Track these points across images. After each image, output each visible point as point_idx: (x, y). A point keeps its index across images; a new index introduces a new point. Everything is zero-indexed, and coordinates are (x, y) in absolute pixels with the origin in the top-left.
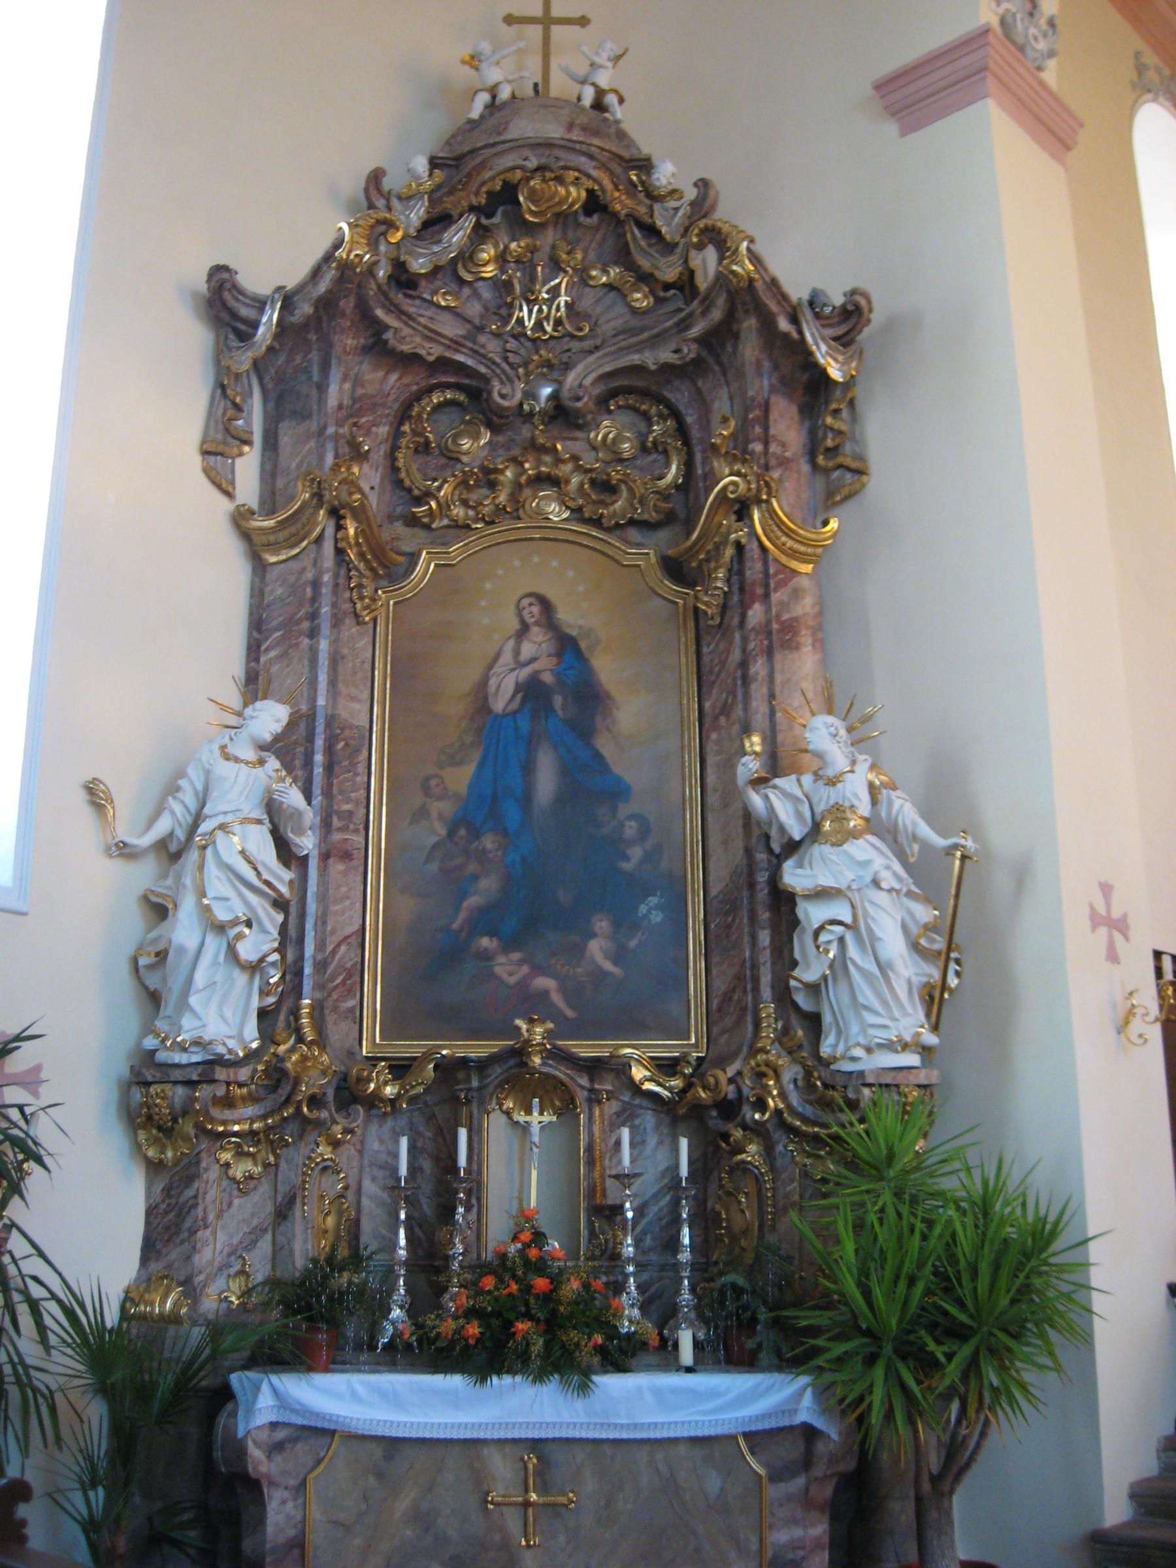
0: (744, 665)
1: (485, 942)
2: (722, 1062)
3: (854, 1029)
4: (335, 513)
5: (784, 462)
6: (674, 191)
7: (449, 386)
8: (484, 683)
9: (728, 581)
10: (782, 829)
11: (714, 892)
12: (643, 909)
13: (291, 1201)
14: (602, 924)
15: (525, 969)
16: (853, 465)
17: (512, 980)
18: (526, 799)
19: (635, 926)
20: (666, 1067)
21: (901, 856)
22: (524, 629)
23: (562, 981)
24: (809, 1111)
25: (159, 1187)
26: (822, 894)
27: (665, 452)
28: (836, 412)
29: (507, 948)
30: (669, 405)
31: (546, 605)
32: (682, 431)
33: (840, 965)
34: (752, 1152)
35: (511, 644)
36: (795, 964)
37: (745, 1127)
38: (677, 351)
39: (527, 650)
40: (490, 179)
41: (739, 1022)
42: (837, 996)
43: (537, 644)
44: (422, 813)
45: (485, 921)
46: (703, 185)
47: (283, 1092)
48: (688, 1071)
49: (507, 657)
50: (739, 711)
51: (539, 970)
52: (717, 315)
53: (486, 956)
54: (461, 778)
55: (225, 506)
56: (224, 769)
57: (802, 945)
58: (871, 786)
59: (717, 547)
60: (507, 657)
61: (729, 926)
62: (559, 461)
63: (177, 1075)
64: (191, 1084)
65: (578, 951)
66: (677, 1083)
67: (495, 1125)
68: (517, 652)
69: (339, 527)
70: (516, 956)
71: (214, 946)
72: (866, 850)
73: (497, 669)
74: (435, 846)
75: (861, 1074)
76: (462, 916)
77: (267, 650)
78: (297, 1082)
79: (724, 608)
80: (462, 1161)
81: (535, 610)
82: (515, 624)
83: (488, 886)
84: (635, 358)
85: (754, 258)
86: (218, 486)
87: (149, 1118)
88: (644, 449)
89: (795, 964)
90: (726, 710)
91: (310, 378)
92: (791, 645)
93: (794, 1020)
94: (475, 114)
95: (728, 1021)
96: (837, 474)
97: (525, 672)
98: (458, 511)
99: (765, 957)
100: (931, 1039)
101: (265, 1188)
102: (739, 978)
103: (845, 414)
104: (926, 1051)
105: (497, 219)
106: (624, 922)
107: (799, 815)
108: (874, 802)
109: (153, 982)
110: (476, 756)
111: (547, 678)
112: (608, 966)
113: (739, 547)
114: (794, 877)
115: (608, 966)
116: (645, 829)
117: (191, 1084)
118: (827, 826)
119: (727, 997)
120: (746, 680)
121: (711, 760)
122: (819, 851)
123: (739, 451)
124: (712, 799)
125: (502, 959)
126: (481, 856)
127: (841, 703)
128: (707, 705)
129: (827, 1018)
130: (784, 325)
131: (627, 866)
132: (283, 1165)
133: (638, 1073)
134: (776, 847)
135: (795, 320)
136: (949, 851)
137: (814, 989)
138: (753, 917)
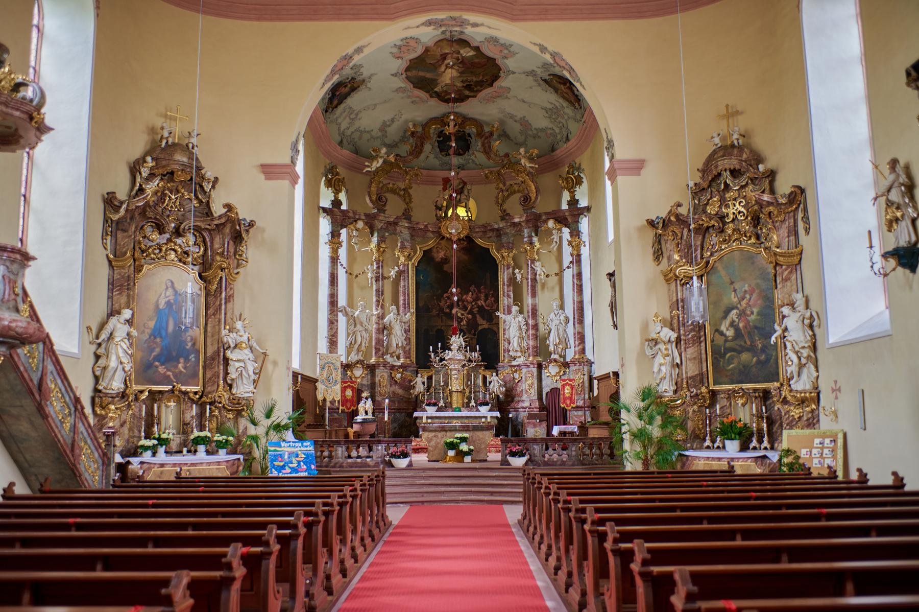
0: (220, 305)
1: (157, 363)
2: (209, 393)
3: (242, 388)
4: (134, 260)
5: (231, 256)
6: (209, 179)
7: (152, 222)
8: (158, 301)
9: (217, 285)
10: (229, 344)
11: (208, 354)
12: (190, 357)
13: (125, 422)
14: (182, 360)
15: (165, 370)
16: (245, 260)
17: (162, 372)
18: (166, 330)
19: (189, 360)
20: (196, 393)
21: (252, 352)
22: (167, 288)
23: (173, 372)
24: (230, 404)
25: (96, 420)
26: (239, 361)
27: (199, 246)
28: (242, 247)
29: (162, 365)
30: (202, 235)
31: (172, 283)
32: (204, 242)
33: (241, 374)
34: (217, 413)
35: (164, 292)
36: (229, 374)
37: (216, 407)
38: (209, 225)
39: (168, 294)
40: (169, 169)
41: (213, 385)
42: (239, 382)
43: (170, 292)
44: (143, 332)
45: (157, 358)
46: (216, 179)
47: (126, 399)
48: (200, 394)
49: (163, 295)
50: (218, 316)
51: (168, 370)
52: (223, 220)
53: (157, 367)
54: (152, 324)
55: (105, 252)
56: (119, 326)
57: (231, 369)
58: (248, 338)
59: (215, 276)
60: (163, 295)
61: (212, 364)
62: (175, 244)
63: (110, 395)
64: (112, 397)
65: (176, 367)
66: (197, 396)
67: (163, 406)
68: (165, 294)
69: (135, 263)
70: (163, 367)
71: (120, 367)
72: (247, 351)
73: (161, 298)
74: (146, 340)
75: (244, 397)
76: (152, 357)
77: (116, 291)
78: (128, 398)
79: (215, 291)
80: (156, 413)
81: (170, 284)
82: (165, 287)
83: (158, 350)
84: (199, 224)
85: (237, 213)
86: (104, 247)
87: (100, 405)
88: (195, 244)
89: (229, 374)
90: (214, 314)
91: (126, 221)
92: (230, 301)
93: (226, 385)
94: (163, 146)
95: (210, 384)
96: (240, 261)
97: (167, 299)
98: (152, 256)
99: (221, 371)
100: (255, 391)
101: (118, 420)
102: (214, 375)
103: (245, 247)
104: (254, 393)
105: (166, 178)
106: (187, 360)
107: (233, 342)
108: (249, 341)
109: (98, 373)
110: (156, 319)
111: (172, 301)
112: (183, 370)
113: (221, 277)
114: (229, 354)
115: (183, 370)
116: (192, 339)
117: (112, 397)
118: (239, 346)
119: (210, 379)
120: (220, 308)
121: (209, 325)
122: (237, 350)
123: (222, 254)
124: (209, 334)
125: (160, 367)
126: (156, 343)
127: (242, 319)
128: (209, 312)
129: (234, 385)
130: (238, 228)
131: (188, 347)
132: (123, 415)
133: (191, 395)
134: (225, 348)
135: (239, 225)
136: (263, 353)
137: (232, 380)
138: (219, 362)
